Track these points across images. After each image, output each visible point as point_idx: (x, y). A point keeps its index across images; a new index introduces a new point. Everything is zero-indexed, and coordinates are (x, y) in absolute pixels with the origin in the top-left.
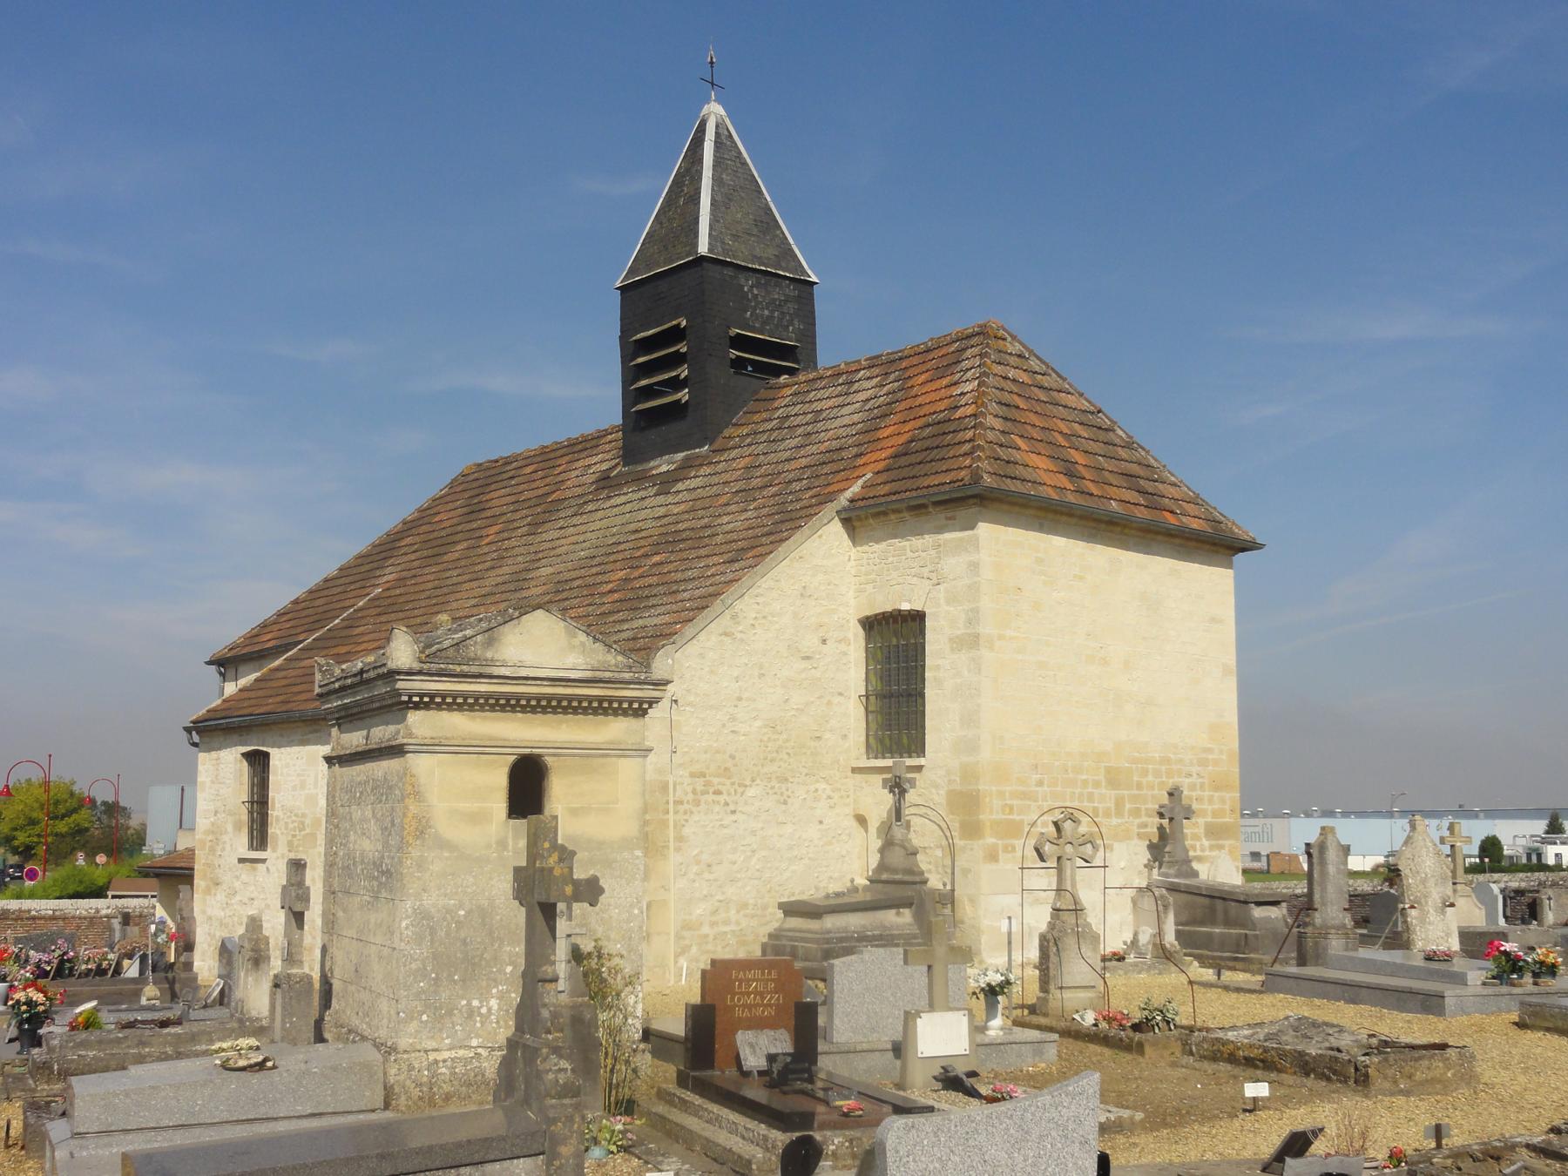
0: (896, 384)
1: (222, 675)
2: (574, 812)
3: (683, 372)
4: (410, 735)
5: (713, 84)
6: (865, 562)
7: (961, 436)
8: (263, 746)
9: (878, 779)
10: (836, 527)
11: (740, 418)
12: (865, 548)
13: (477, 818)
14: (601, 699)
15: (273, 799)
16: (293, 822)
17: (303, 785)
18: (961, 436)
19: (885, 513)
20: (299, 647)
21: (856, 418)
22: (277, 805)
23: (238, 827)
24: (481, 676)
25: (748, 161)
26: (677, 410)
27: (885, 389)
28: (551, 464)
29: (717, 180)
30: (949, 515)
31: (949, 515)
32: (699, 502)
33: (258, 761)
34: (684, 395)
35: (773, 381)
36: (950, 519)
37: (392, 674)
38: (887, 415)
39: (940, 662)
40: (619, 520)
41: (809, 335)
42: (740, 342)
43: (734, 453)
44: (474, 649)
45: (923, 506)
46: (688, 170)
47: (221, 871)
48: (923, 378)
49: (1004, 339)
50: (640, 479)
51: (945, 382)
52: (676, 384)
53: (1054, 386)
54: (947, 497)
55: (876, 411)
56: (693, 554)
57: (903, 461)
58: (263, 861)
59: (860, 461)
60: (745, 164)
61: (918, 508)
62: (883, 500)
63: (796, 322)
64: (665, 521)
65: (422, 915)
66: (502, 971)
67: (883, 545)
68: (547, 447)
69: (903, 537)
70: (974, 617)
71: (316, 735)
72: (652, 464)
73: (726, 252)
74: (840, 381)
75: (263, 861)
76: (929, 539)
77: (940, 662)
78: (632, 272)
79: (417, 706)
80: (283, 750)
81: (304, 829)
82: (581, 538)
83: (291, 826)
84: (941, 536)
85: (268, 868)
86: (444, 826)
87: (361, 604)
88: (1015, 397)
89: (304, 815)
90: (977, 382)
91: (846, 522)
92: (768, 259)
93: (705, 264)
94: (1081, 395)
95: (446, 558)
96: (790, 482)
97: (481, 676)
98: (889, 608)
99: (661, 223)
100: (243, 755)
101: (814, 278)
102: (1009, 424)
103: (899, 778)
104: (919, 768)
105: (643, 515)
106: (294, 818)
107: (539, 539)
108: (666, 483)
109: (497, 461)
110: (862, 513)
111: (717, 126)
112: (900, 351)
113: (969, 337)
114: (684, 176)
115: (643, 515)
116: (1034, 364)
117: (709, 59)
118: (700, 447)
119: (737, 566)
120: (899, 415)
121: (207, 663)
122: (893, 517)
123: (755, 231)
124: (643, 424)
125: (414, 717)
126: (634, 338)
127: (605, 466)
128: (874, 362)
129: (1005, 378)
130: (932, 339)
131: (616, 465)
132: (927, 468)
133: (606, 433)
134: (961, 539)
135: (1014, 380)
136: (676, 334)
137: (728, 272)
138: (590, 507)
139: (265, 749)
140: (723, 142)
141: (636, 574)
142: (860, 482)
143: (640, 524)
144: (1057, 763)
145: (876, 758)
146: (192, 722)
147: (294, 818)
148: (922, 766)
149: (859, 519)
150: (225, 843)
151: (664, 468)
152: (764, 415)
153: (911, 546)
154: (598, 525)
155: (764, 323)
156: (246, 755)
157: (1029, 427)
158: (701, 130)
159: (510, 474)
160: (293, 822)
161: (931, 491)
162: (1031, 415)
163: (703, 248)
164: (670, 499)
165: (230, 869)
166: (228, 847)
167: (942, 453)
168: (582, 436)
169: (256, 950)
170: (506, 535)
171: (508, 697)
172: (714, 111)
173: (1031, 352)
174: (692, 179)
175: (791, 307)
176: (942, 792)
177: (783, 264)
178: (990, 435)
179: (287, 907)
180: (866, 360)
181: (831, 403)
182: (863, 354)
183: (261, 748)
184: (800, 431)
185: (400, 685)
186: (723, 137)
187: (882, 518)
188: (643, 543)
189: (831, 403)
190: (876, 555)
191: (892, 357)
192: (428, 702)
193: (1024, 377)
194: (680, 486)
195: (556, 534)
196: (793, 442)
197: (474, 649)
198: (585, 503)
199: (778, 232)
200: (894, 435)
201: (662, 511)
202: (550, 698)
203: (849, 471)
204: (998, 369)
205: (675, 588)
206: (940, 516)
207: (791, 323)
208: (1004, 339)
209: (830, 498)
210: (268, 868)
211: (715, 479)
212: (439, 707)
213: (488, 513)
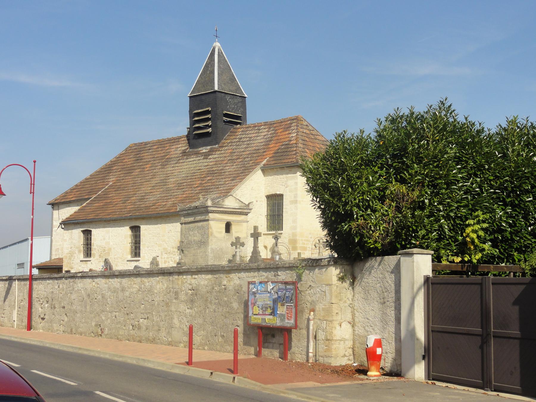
0: (273, 131)
1: (53, 208)
2: (236, 232)
3: (210, 123)
4: (210, 218)
5: (217, 37)
6: (267, 181)
7: (292, 149)
9: (271, 236)
10: (260, 172)
11: (226, 137)
12: (267, 177)
13: (220, 232)
14: (241, 212)
15: (93, 243)
16: (101, 249)
17: (104, 239)
18: (292, 149)
19: (273, 169)
21: (262, 140)
22: (95, 245)
23: (80, 251)
24: (222, 207)
25: (227, 60)
26: (208, 134)
27: (270, 133)
28: (163, 146)
29: (219, 67)
32: (217, 162)
33: (87, 234)
34: (210, 130)
35: (235, 126)
36: (290, 171)
37: (207, 207)
38: (271, 141)
40: (193, 166)
41: (244, 113)
42: (226, 115)
43: (226, 148)
44: (220, 203)
45: (284, 167)
46: (210, 63)
47: (74, 264)
48: (281, 130)
49: (303, 121)
50: (197, 154)
51: (287, 132)
52: (208, 126)
53: (316, 134)
54: (290, 166)
55: (268, 139)
56: (220, 177)
57: (277, 155)
58: (90, 261)
59: (265, 154)
60: (226, 61)
61: (282, 168)
62: (273, 165)
63: (241, 109)
64: (207, 167)
65: (212, 249)
66: (225, 259)
67: (272, 177)
68: (160, 140)
69: (278, 175)
70: (296, 196)
72: (200, 149)
73: (222, 89)
74: (256, 129)
75: (90, 261)
76: (284, 176)
78: (192, 92)
79: (211, 213)
80: (96, 229)
81: (105, 251)
82: (181, 171)
83: (100, 251)
85: (91, 263)
86: (215, 234)
87: (106, 187)
88: (306, 138)
89: (104, 247)
90: (296, 134)
91: (263, 171)
92: (233, 90)
93: (217, 93)
94: (323, 136)
96: (245, 158)
97: (222, 207)
99: (202, 78)
100: (81, 231)
101: (246, 96)
102: (304, 145)
104: (281, 234)
105: (200, 164)
106: (101, 248)
107: (166, 170)
108: (206, 156)
109: (142, 143)
111: (218, 50)
112: (273, 121)
113: (293, 120)
114: (208, 64)
115: (200, 164)
116: (310, 128)
117: (216, 29)
118: (215, 145)
119: (234, 181)
120: (275, 141)
121: (47, 204)
122: (275, 170)
123: (230, 82)
124: (196, 137)
125: (210, 214)
126: (194, 112)
127: (183, 148)
128: (266, 124)
129: (303, 132)
130: (282, 119)
131: (187, 148)
132: (284, 157)
133: (181, 137)
135: (305, 133)
136: (207, 112)
137: (223, 95)
138: (181, 161)
140: (220, 55)
141: (204, 182)
142: (266, 160)
143: (200, 167)
144: (315, 233)
145: (269, 231)
147: (101, 248)
148: (282, 233)
149: (266, 170)
151: (204, 151)
152: (234, 137)
154: (186, 167)
155: (233, 109)
156: (84, 232)
157: (309, 146)
158: (214, 51)
159: (149, 148)
161: (286, 164)
162: (310, 143)
163: (216, 88)
164: (208, 160)
165: (77, 264)
166: (76, 258)
167: (288, 153)
168: (173, 138)
169: (156, 263)
170: (153, 168)
171: (225, 211)
172: (217, 45)
173: (309, 124)
174: (211, 66)
175: (240, 104)
176: (287, 239)
177: (238, 92)
178: (300, 149)
179: (180, 250)
181: (254, 135)
182: (262, 121)
184: (246, 143)
185: (209, 209)
186: (220, 53)
187: (272, 170)
188: (203, 173)
189: (254, 135)
191: (271, 123)
192: (213, 212)
193: (308, 132)
194: (210, 157)
195: (172, 169)
196: (244, 146)
197: (220, 203)
198: (179, 160)
199: (236, 82)
200: (274, 147)
201: (206, 164)
202: (232, 211)
203: (263, 157)
204: (301, 130)
205: (217, 187)
207: (240, 109)
208: (303, 121)
209: (257, 164)
210: (91, 263)
211: (221, 156)
212: (214, 213)
213: (145, 160)
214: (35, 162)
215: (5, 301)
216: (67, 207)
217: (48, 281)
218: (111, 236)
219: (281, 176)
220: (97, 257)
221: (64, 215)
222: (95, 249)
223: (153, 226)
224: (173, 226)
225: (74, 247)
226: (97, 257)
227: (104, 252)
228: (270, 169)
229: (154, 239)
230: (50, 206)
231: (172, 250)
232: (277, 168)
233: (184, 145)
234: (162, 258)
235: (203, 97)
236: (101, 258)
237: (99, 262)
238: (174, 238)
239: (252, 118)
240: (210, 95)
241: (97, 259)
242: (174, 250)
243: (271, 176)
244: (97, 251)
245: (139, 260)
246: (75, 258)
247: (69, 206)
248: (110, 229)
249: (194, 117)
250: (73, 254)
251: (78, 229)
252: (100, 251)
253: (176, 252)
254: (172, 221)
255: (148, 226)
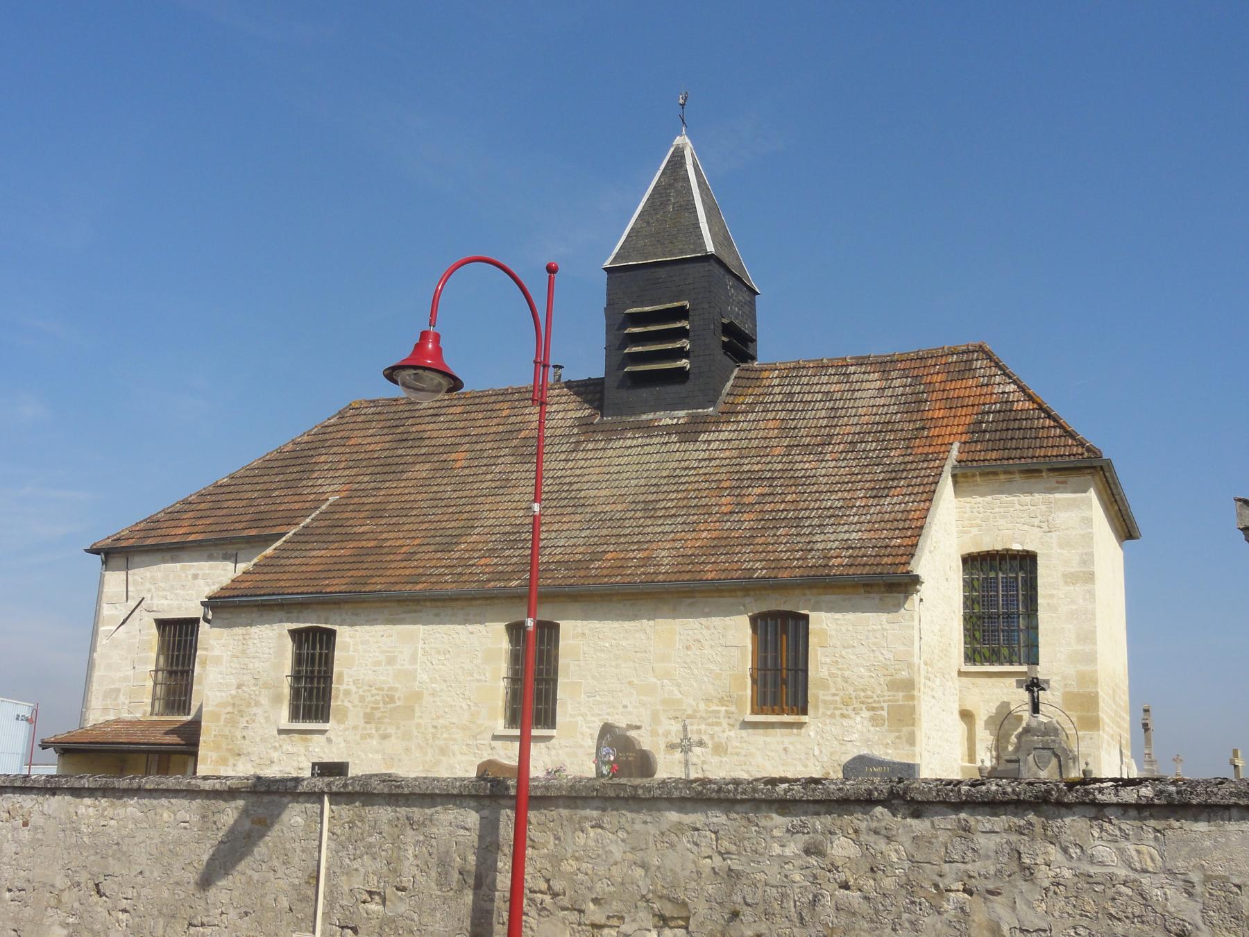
1: (105, 562)
3: (685, 344)
8: (326, 623)
9: (1013, 681)
12: (969, 499)
15: (341, 674)
16: (372, 696)
19: (995, 473)
20: (284, 539)
23: (277, 699)
30: (1060, 480)
31: (1060, 480)
34: (684, 363)
39: (1054, 592)
45: (1040, 471)
47: (247, 742)
52: (680, 353)
54: (1071, 465)
58: (323, 732)
61: (1031, 472)
67: (989, 498)
69: (1010, 493)
71: (414, 614)
75: (323, 732)
77: (1054, 592)
80: (358, 628)
83: (369, 699)
84: (1051, 496)
85: (329, 740)
89: (390, 689)
95: (405, 476)
98: (999, 547)
99: (648, 223)
103: (1037, 679)
106: (374, 692)
108: (688, 433)
110: (969, 472)
118: (704, 409)
121: (87, 551)
122: (1002, 477)
124: (629, 383)
134: (1074, 500)
136: (681, 313)
139: (329, 626)
146: (206, 597)
147: (374, 692)
150: (255, 715)
153: (1018, 500)
160: (372, 696)
163: (710, 248)
165: (263, 740)
180: (851, 358)
183: (324, 626)
187: (991, 477)
190: (980, 505)
194: (703, 437)
206: (1052, 480)
210: (329, 740)
214: (551, 270)
215: (206, 882)
216: (166, 562)
217: (673, 816)
218: (420, 652)
219: (1027, 498)
220: (355, 716)
221: (148, 585)
222: (347, 693)
223: (616, 624)
224: (708, 628)
225: (255, 685)
226: (355, 716)
227: (385, 703)
228: (982, 474)
229: (617, 666)
230: (98, 559)
231: (702, 706)
232: (1010, 473)
233: (572, 406)
234: (654, 733)
235: (662, 273)
236: (373, 725)
237: (363, 737)
238: (711, 666)
239: (767, 349)
240: (687, 266)
241: (355, 728)
242: (715, 708)
243: (982, 495)
244: (356, 701)
245: (550, 738)
246: (254, 721)
247: (174, 560)
248: (421, 628)
249: (624, 326)
250: (249, 705)
251: (275, 626)
252: (369, 699)
253: (722, 715)
254: (707, 610)
255: (595, 624)
